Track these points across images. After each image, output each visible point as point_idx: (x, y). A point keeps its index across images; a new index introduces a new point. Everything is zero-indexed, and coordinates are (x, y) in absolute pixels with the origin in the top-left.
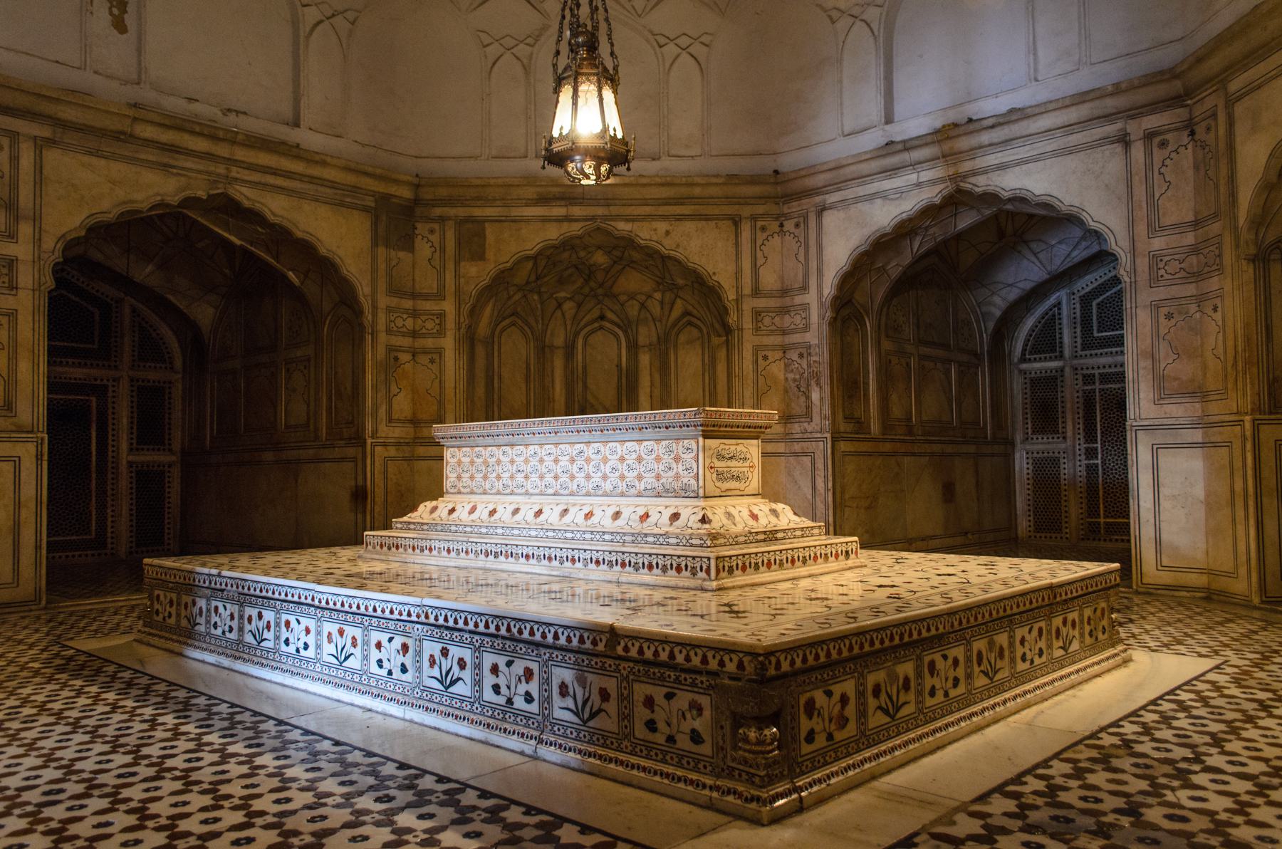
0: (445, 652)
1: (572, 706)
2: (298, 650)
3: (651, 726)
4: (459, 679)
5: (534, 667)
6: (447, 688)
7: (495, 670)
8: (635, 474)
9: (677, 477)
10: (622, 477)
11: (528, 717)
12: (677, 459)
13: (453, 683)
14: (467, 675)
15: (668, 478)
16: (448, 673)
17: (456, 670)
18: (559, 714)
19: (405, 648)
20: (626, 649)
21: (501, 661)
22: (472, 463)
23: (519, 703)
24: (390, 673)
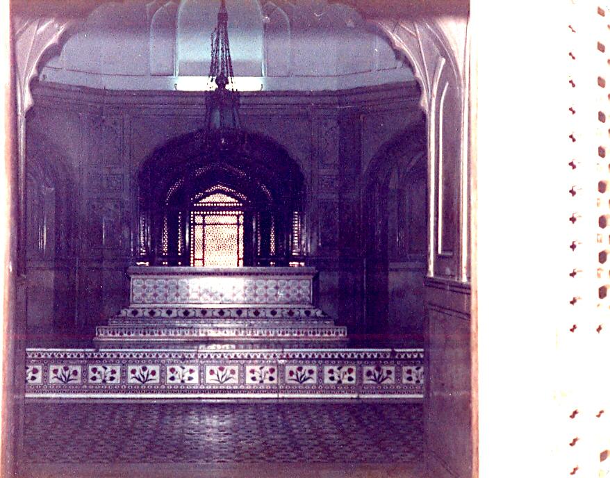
0: (300, 369)
1: (372, 377)
2: (183, 381)
3: (410, 379)
4: (309, 378)
5: (354, 368)
6: (301, 383)
7: (331, 371)
8: (274, 294)
9: (299, 295)
10: (266, 296)
11: (350, 386)
12: (299, 288)
13: (305, 380)
14: (314, 376)
15: (293, 296)
16: (301, 377)
17: (307, 375)
18: (365, 382)
19: (272, 371)
20: (399, 356)
21: (335, 368)
22: (155, 287)
23: (345, 381)
24: (261, 382)
